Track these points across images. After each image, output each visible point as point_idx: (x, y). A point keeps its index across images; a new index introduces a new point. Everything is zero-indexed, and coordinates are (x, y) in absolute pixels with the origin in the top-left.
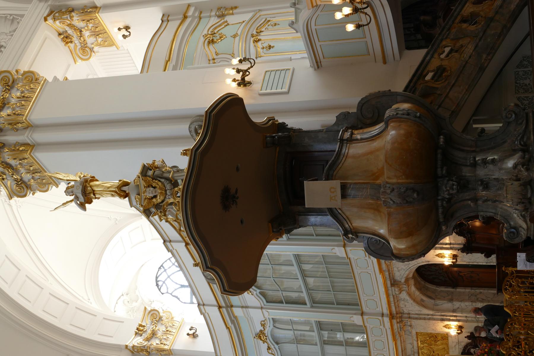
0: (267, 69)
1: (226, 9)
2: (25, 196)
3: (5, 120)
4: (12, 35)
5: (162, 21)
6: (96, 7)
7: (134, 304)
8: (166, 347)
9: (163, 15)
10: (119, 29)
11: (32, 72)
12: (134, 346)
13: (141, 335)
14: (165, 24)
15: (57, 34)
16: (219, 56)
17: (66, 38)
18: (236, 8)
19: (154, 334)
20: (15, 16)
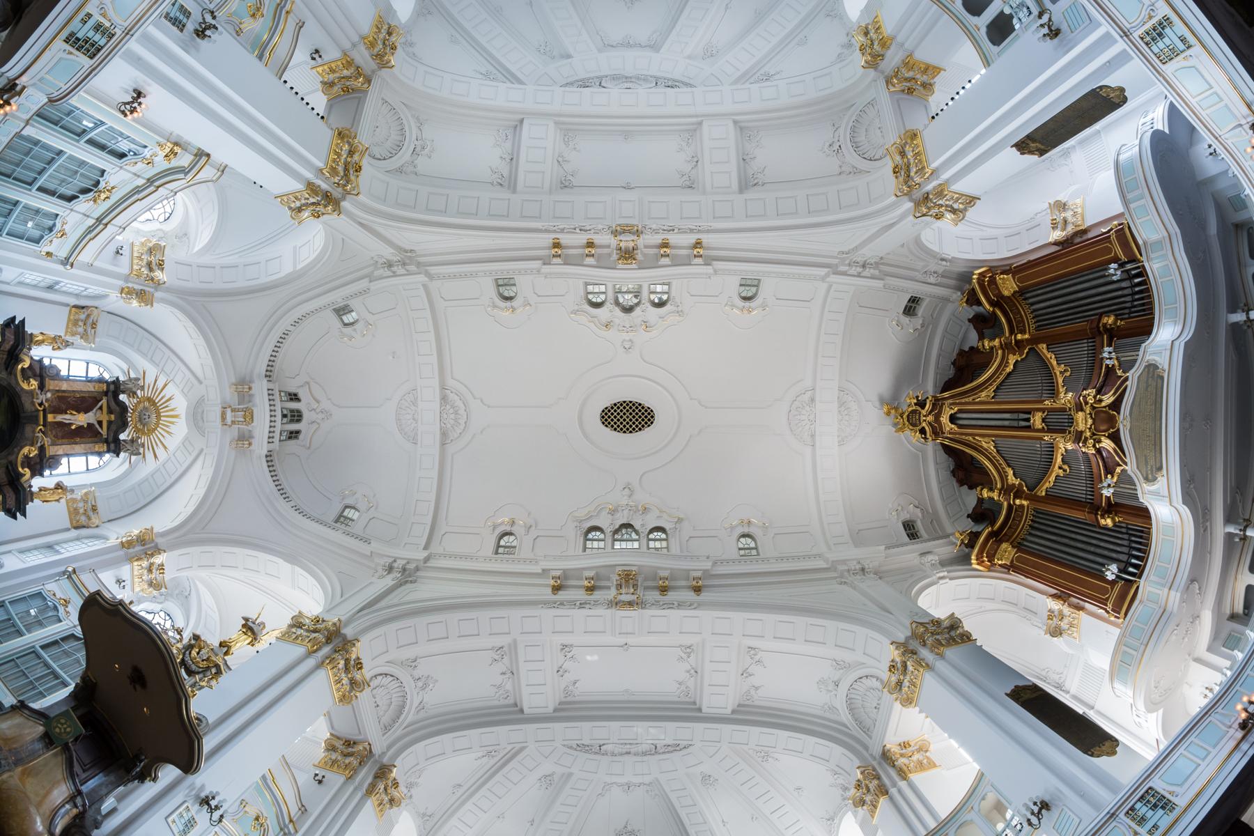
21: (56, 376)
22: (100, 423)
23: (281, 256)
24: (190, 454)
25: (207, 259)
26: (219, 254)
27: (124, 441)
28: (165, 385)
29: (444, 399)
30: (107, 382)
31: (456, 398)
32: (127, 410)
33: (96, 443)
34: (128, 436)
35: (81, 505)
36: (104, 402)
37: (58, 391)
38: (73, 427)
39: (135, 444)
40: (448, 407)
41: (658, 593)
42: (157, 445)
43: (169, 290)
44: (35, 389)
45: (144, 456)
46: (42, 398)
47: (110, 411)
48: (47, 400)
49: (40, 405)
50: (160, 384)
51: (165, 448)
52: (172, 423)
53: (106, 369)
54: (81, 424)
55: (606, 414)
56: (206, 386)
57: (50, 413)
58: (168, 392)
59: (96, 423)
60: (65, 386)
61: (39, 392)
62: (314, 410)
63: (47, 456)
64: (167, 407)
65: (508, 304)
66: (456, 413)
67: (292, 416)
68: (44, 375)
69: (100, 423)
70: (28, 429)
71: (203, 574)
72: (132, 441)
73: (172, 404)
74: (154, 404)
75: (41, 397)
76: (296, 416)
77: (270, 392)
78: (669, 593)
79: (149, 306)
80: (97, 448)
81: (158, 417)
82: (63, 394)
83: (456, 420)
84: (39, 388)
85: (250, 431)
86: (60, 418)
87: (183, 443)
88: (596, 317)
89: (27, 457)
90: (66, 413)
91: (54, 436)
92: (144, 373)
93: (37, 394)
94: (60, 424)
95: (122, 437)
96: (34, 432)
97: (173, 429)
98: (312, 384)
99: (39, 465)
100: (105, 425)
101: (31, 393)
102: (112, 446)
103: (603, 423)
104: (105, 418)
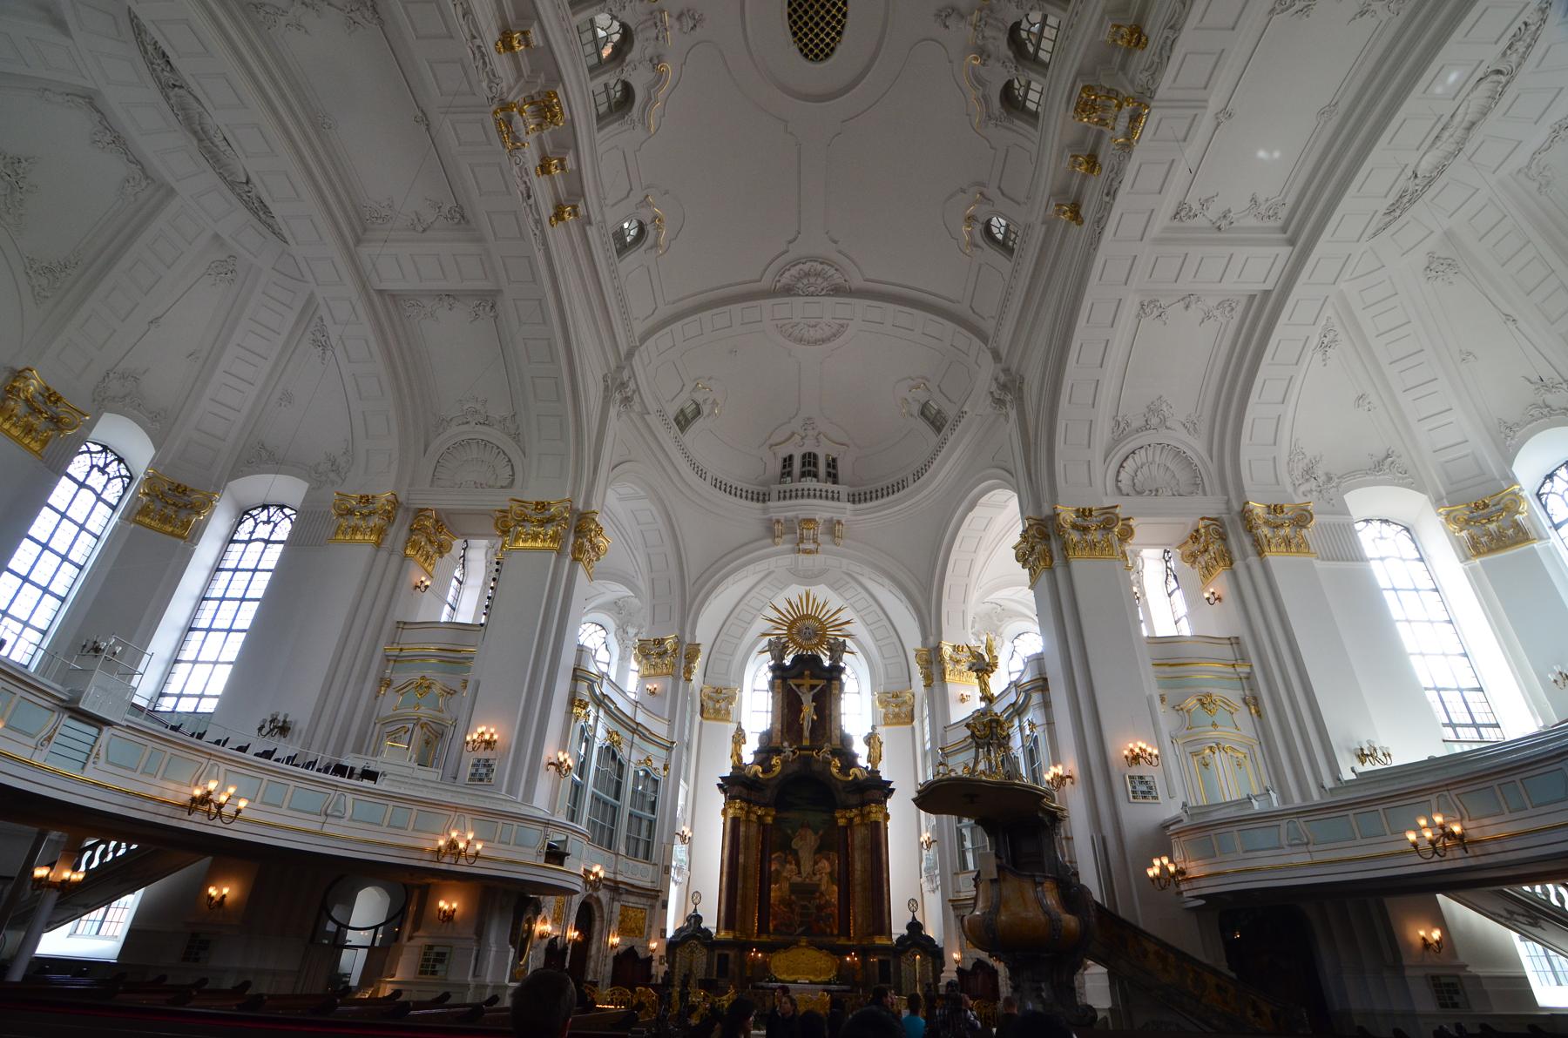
0: (1155, 778)
1: (1256, 705)
2: (1018, 561)
3: (1068, 539)
4: (1174, 495)
5: (1229, 639)
6: (1231, 564)
7: (995, 618)
8: (947, 677)
9: (1237, 638)
10: (1213, 593)
11: (1132, 530)
12: (942, 648)
13: (954, 651)
14: (1228, 642)
15: (1196, 529)
16: (1186, 715)
17: (1195, 536)
18: (1260, 716)
19: (958, 662)
20: (1200, 486)
21: (766, 737)
22: (813, 687)
23: (632, 511)
24: (848, 583)
25: (643, 585)
26: (636, 571)
28: (776, 609)
29: (788, 291)
30: (774, 678)
31: (787, 274)
32: (802, 655)
33: (831, 692)
34: (825, 655)
35: (891, 709)
36: (791, 683)
37: (782, 732)
38: (815, 717)
39: (834, 648)
40: (800, 285)
41: (1138, 53)
42: (836, 620)
43: (682, 631)
44: (780, 759)
46: (788, 751)
47: (800, 675)
48: (790, 746)
49: (794, 752)
50: (774, 615)
51: (840, 610)
52: (814, 600)
53: (758, 670)
54: (812, 710)
55: (811, 51)
56: (776, 567)
57: (802, 742)
58: (783, 606)
59: (812, 693)
60: (778, 726)
62: (802, 438)
63: (839, 747)
64: (797, 606)
65: (650, 228)
66: (807, 275)
67: (809, 465)
69: (813, 687)
71: (974, 596)
72: (830, 649)
73: (795, 600)
74: (795, 621)
76: (810, 460)
77: (782, 495)
78: (1146, 31)
79: (700, 648)
81: (807, 617)
82: (785, 727)
83: (817, 275)
84: (779, 755)
85: (825, 521)
86: (806, 733)
88: (649, 93)
89: (840, 770)
90: (802, 724)
91: (823, 737)
94: (812, 731)
95: (827, 663)
97: (820, 600)
98: (771, 441)
99: (849, 759)
100: (815, 682)
101: (784, 762)
102: (835, 674)
103: (827, 55)
104: (808, 682)
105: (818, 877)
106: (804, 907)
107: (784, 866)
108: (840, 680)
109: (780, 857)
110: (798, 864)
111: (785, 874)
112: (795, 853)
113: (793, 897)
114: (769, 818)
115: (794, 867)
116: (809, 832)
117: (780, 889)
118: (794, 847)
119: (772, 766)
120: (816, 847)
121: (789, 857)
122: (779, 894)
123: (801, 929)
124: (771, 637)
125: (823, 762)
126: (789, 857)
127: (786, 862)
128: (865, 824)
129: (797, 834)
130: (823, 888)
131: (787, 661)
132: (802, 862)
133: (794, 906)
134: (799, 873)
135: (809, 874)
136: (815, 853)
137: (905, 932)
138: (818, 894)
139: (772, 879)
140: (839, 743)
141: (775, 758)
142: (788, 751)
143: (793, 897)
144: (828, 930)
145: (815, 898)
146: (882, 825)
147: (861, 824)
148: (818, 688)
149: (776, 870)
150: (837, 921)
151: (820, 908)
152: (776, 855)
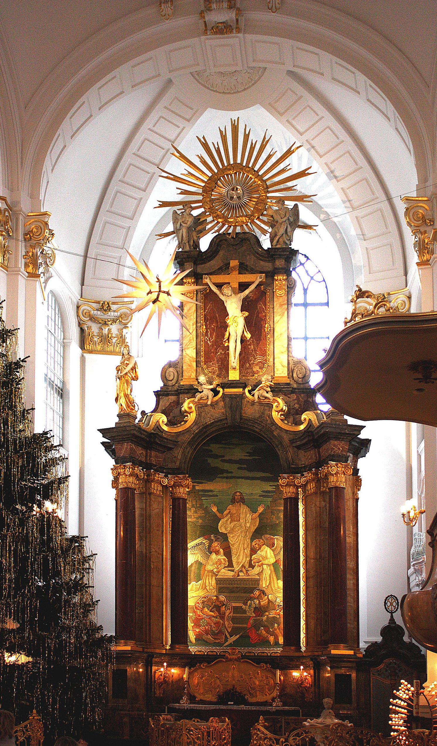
27: (272, 241)
28: (183, 157)
37: (198, 363)
45: (302, 198)
47: (225, 269)
49: (215, 392)
51: (289, 153)
52: (246, 137)
60: (191, 353)
61: (198, 395)
64: (218, 151)
68: (175, 388)
69: (243, 286)
70: (249, 412)
75: (206, 392)
80: (280, 293)
81: (238, 167)
87: (281, 114)
90: (228, 346)
91: (261, 368)
92: (164, 204)
93: (201, 398)
95: (266, 244)
96: (253, 403)
97: (256, 138)
100: (245, 278)
102: (280, 263)
105: (257, 570)
106: (236, 610)
107: (208, 557)
108: (288, 273)
109: (201, 543)
110: (228, 554)
111: (209, 567)
112: (225, 537)
113: (222, 598)
114: (182, 490)
115: (222, 557)
116: (244, 509)
117: (204, 587)
118: (222, 530)
119: (183, 415)
120: (253, 529)
121: (215, 544)
122: (201, 593)
123: (234, 638)
124: (176, 208)
125: (260, 403)
126: (215, 544)
127: (210, 550)
128: (323, 492)
129: (225, 513)
130: (264, 584)
131: (204, 244)
132: (234, 551)
133: (223, 608)
134: (231, 565)
135: (243, 566)
136: (252, 539)
137: (379, 639)
138: (257, 593)
139: (191, 575)
140: (286, 375)
141: (187, 401)
142: (206, 391)
143: (222, 598)
144: (272, 639)
145: (252, 599)
146: (348, 493)
147: (316, 493)
148: (252, 287)
149: (197, 562)
150: (282, 626)
151: (260, 611)
152: (197, 541)
